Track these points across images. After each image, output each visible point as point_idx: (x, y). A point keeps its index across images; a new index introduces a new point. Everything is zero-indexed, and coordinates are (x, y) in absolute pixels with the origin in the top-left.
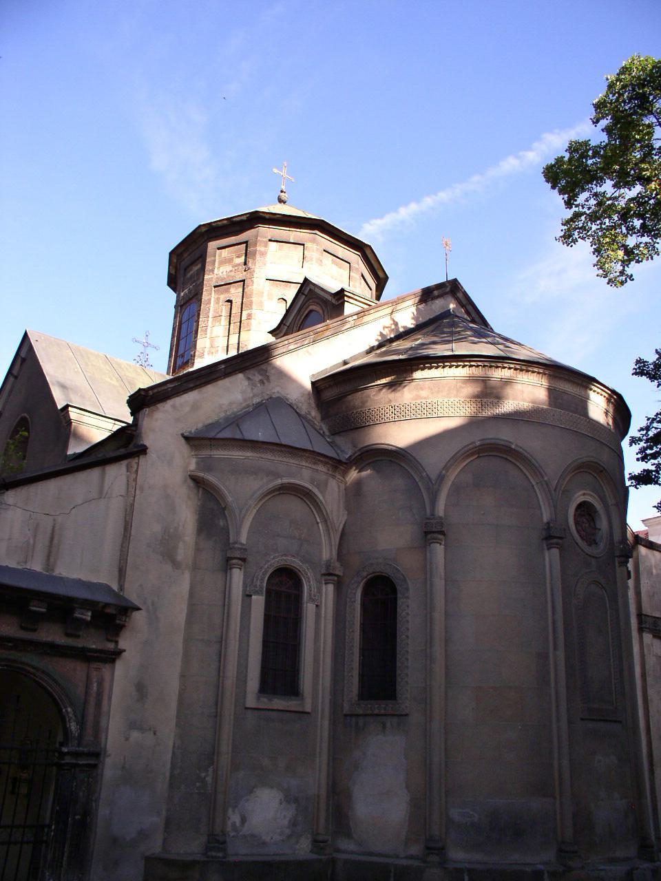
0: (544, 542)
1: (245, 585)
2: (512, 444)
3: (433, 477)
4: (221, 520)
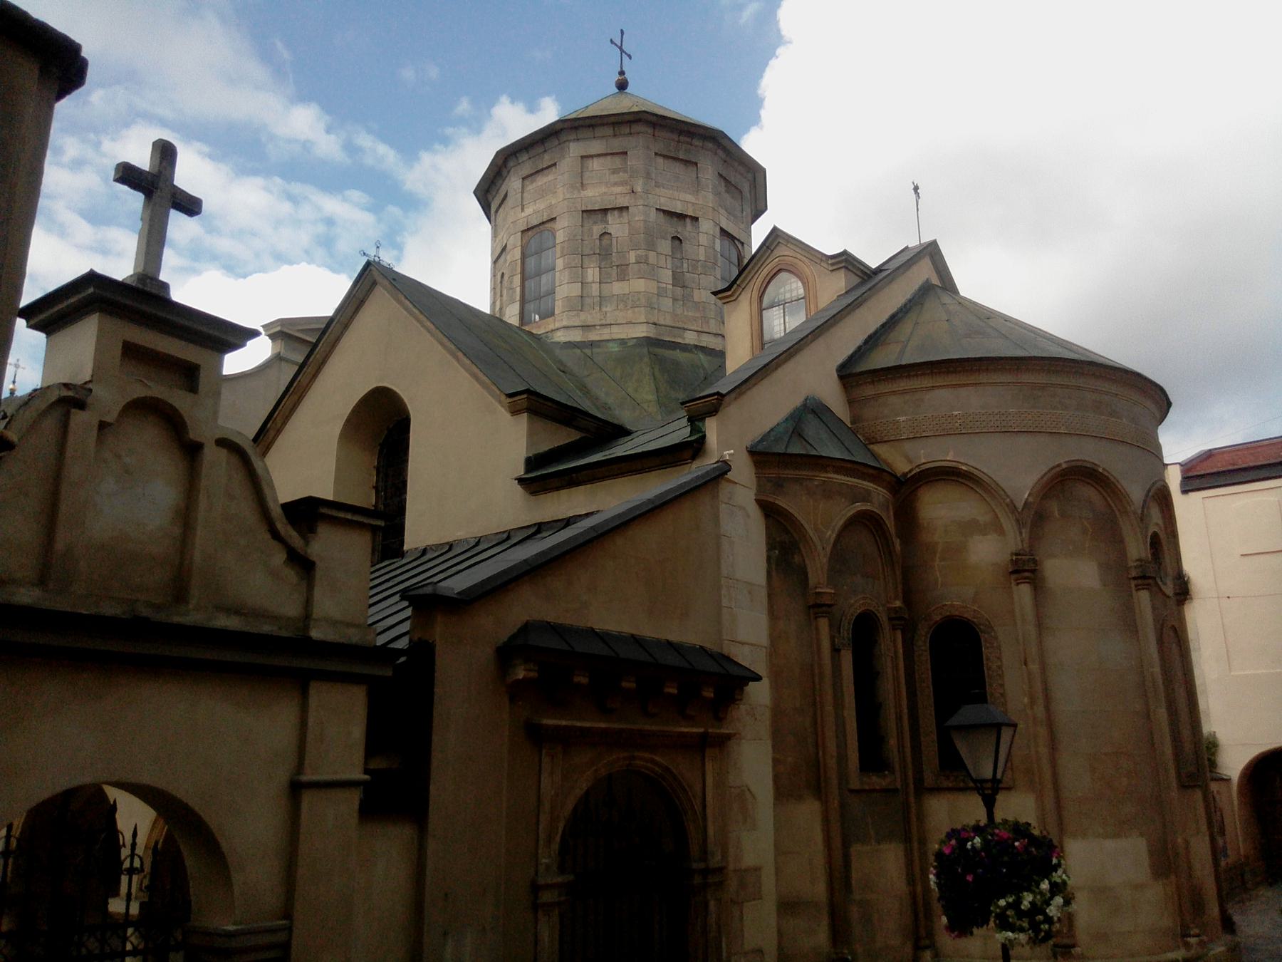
0: (1133, 583)
1: (832, 638)
2: (1099, 466)
3: (1020, 506)
4: (796, 556)
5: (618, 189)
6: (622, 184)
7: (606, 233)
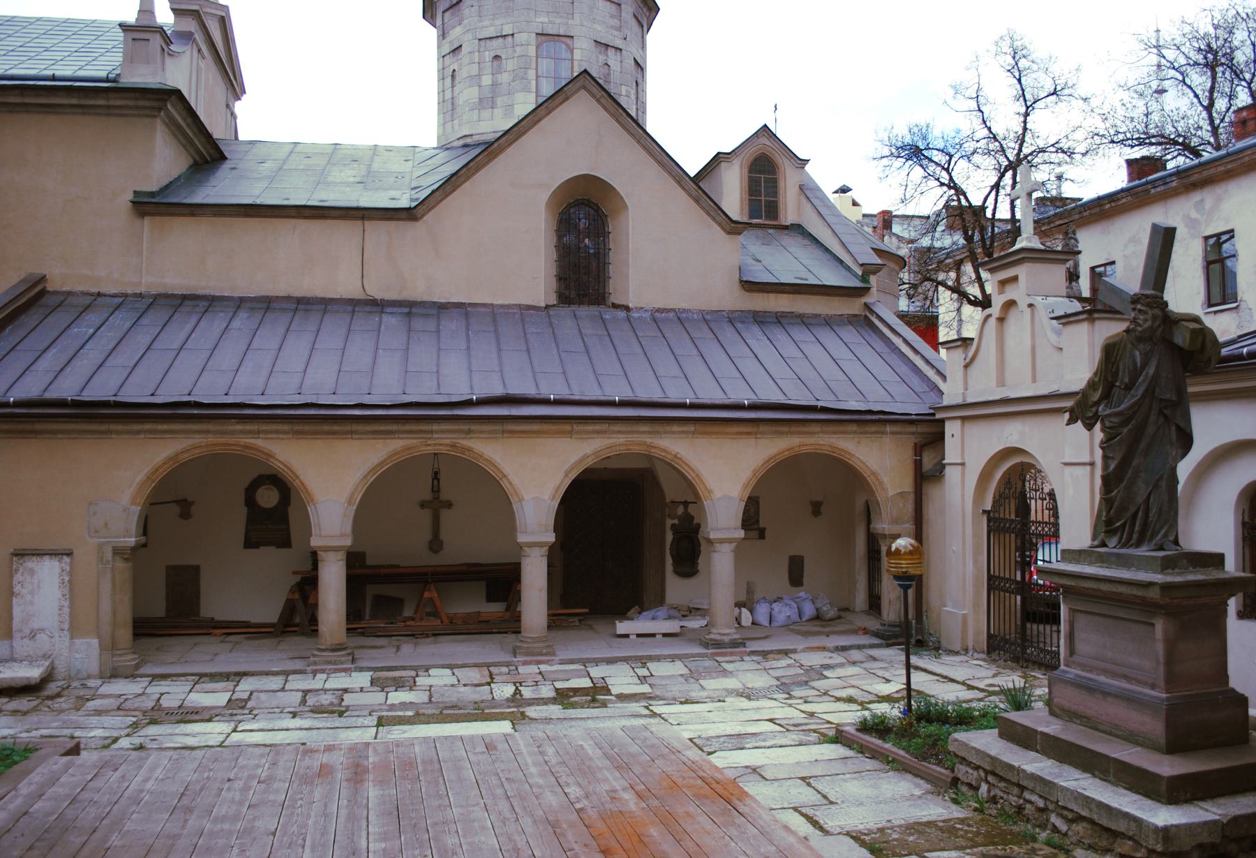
5: (616, 33)
6: (619, 29)
7: (606, 64)
